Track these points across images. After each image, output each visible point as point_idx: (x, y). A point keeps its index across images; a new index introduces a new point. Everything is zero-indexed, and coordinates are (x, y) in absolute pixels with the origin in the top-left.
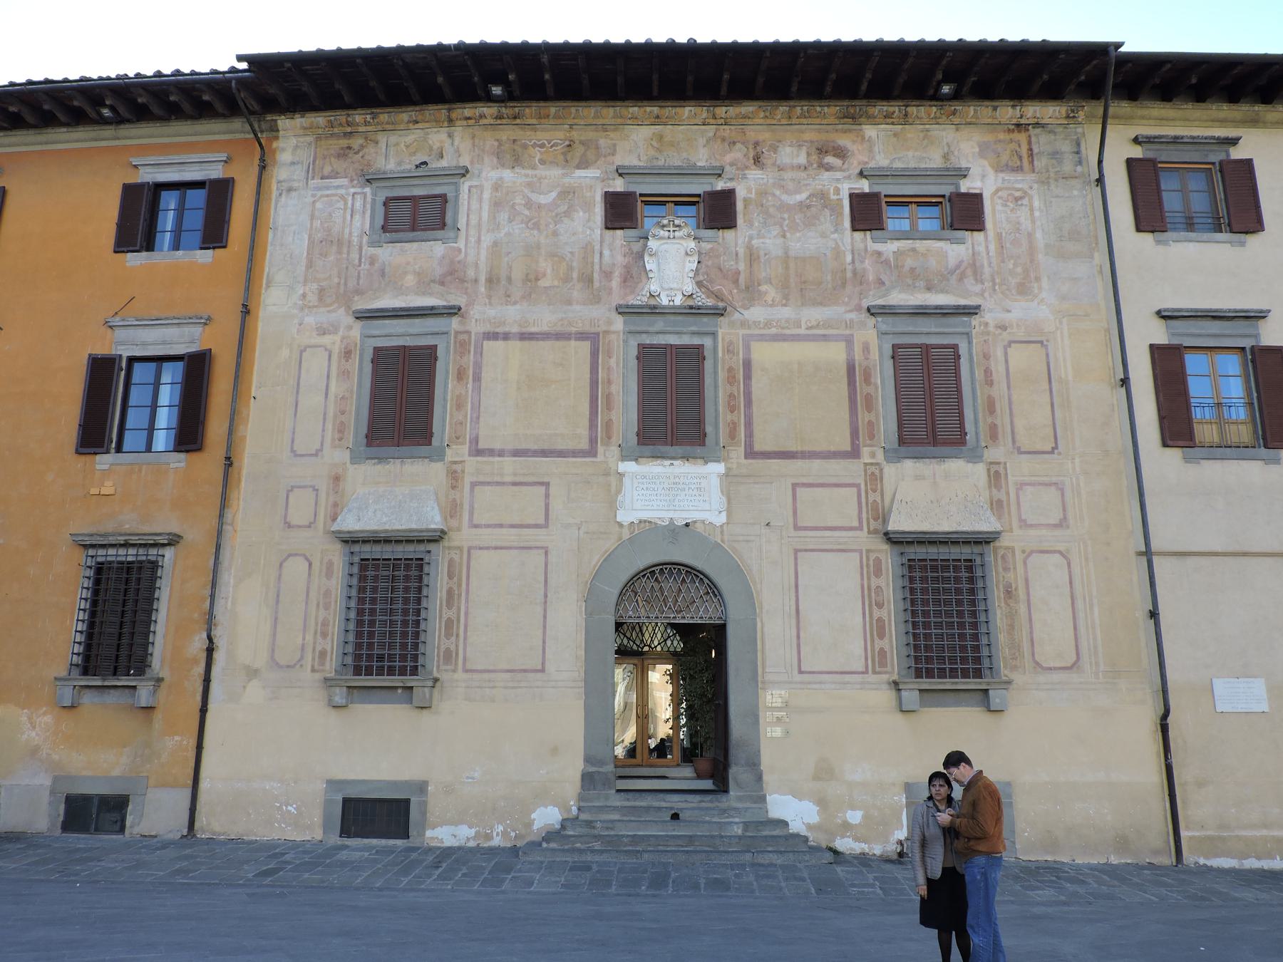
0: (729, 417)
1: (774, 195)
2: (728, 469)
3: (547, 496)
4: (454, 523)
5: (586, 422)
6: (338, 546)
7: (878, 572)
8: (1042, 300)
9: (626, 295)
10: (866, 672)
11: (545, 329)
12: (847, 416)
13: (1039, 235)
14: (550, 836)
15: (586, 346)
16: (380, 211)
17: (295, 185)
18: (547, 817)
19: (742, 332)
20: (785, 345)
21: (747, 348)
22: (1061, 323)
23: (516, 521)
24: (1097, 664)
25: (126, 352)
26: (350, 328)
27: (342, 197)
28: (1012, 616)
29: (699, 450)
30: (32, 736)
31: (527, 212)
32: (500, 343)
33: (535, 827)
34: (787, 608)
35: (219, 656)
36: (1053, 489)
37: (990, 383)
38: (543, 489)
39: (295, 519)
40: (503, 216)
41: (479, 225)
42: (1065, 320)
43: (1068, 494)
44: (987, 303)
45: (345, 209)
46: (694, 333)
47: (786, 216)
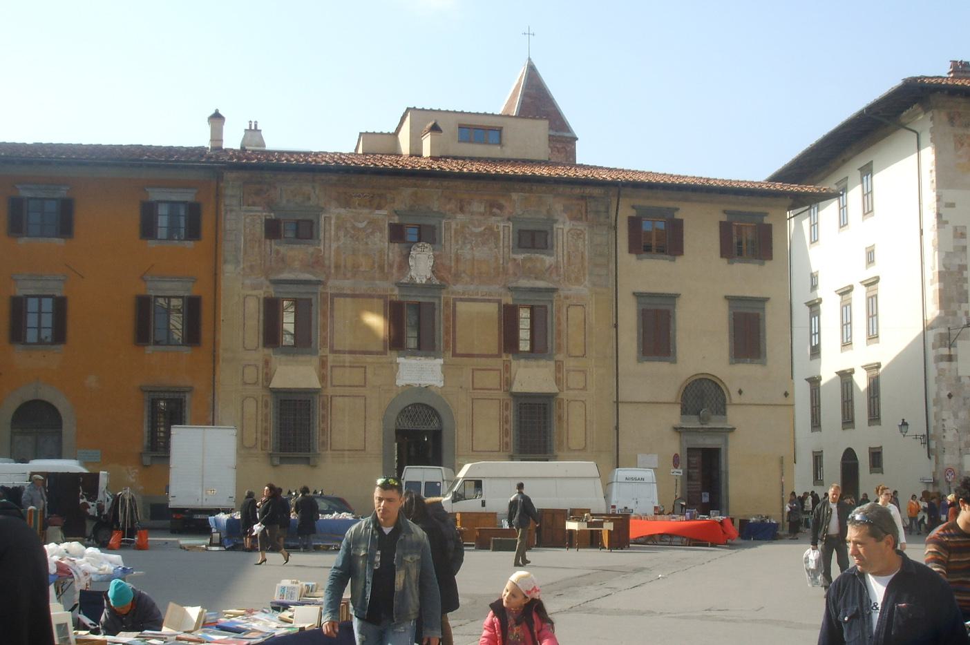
1: (468, 227)
2: (444, 362)
7: (507, 408)
13: (586, 253)
17: (234, 208)
25: (153, 294)
37: (560, 324)
42: (594, 296)
47: (474, 239)
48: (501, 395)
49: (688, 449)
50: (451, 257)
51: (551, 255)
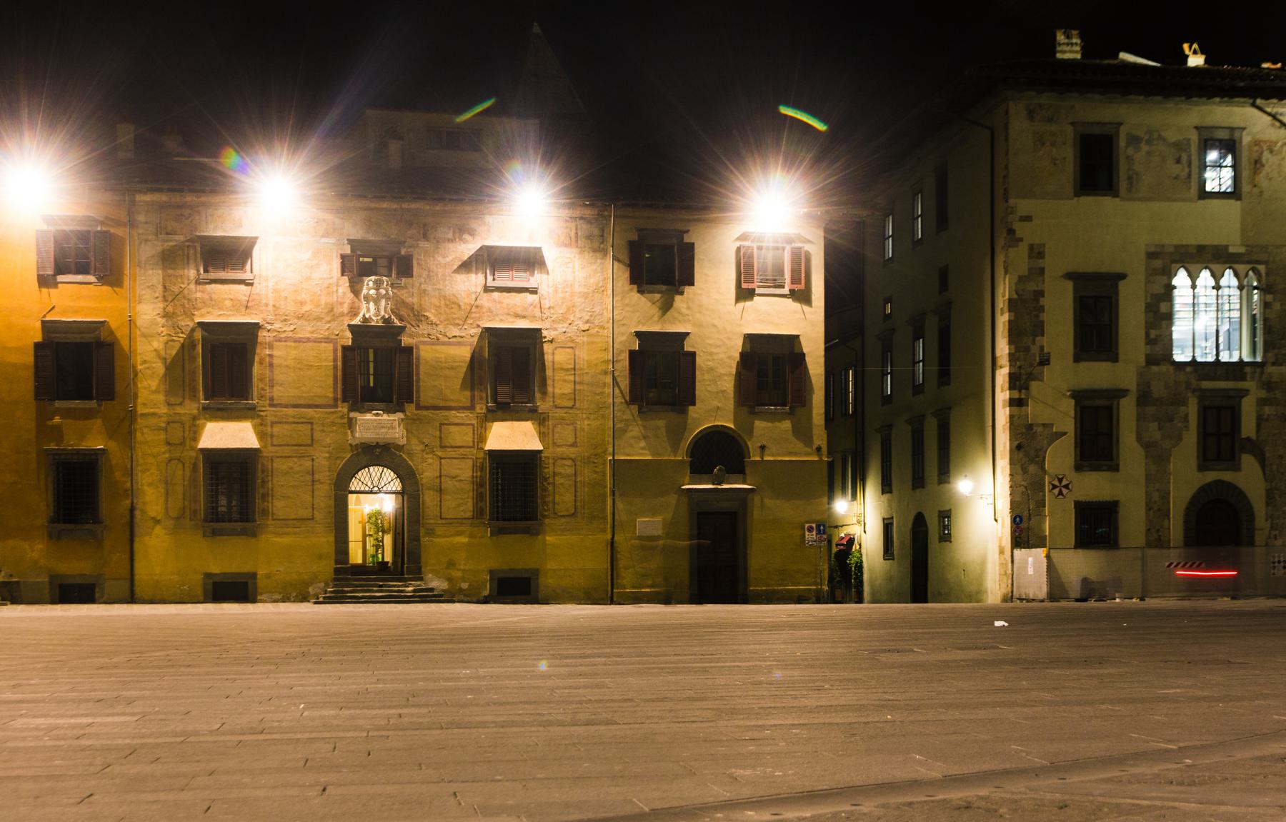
30: (35, 555)
49: (699, 513)
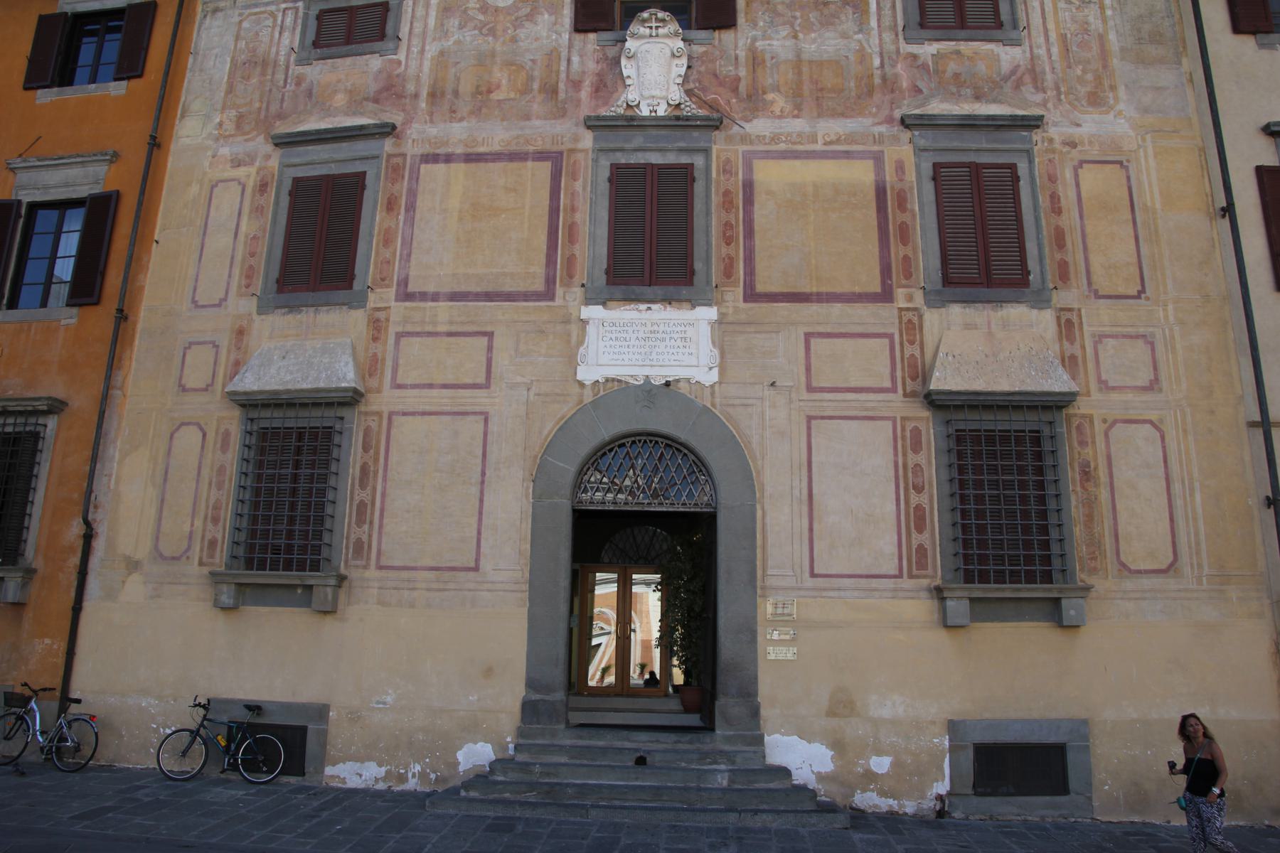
0: (724, 250)
2: (722, 315)
3: (490, 348)
4: (373, 383)
5: (542, 258)
6: (237, 413)
7: (916, 446)
8: (1120, 113)
9: (597, 106)
10: (900, 576)
11: (496, 148)
12: (876, 250)
13: (1112, 36)
14: (480, 779)
15: (545, 168)
16: (313, 24)
18: (475, 754)
19: (742, 148)
20: (797, 163)
21: (749, 168)
22: (1144, 140)
23: (450, 379)
24: (1200, 566)
25: (27, 197)
26: (268, 157)
27: (273, 15)
28: (1090, 503)
29: (684, 291)
31: (481, 17)
32: (441, 167)
33: (461, 768)
34: (796, 492)
35: (99, 545)
36: (1140, 342)
37: (1057, 211)
38: (485, 340)
39: (190, 382)
40: (454, 22)
41: (424, 33)
42: (1148, 137)
43: (1160, 348)
44: (1053, 115)
45: (274, 27)
46: (681, 150)
47: (798, 14)
48: (897, 404)
50: (736, 58)
51: (1016, 43)
